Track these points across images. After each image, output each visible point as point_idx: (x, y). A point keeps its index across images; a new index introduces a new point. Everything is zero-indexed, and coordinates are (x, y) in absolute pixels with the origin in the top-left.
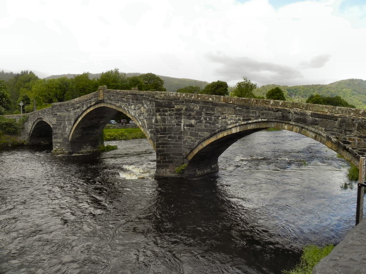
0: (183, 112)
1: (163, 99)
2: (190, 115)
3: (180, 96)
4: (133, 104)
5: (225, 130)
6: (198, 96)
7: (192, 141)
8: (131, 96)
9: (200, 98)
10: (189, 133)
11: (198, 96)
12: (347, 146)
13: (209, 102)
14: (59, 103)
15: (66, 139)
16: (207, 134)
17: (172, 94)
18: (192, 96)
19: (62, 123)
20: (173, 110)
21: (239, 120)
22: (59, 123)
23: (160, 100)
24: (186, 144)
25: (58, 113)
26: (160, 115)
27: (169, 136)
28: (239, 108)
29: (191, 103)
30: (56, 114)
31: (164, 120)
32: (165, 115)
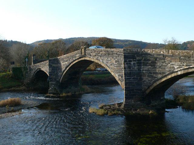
0: (142, 61)
1: (128, 53)
2: (147, 63)
3: (140, 51)
5: (173, 72)
7: (149, 81)
9: (154, 52)
11: (153, 51)
13: (160, 54)
15: (58, 82)
17: (135, 50)
21: (183, 65)
23: (127, 54)
24: (145, 83)
27: (133, 78)
29: (148, 55)
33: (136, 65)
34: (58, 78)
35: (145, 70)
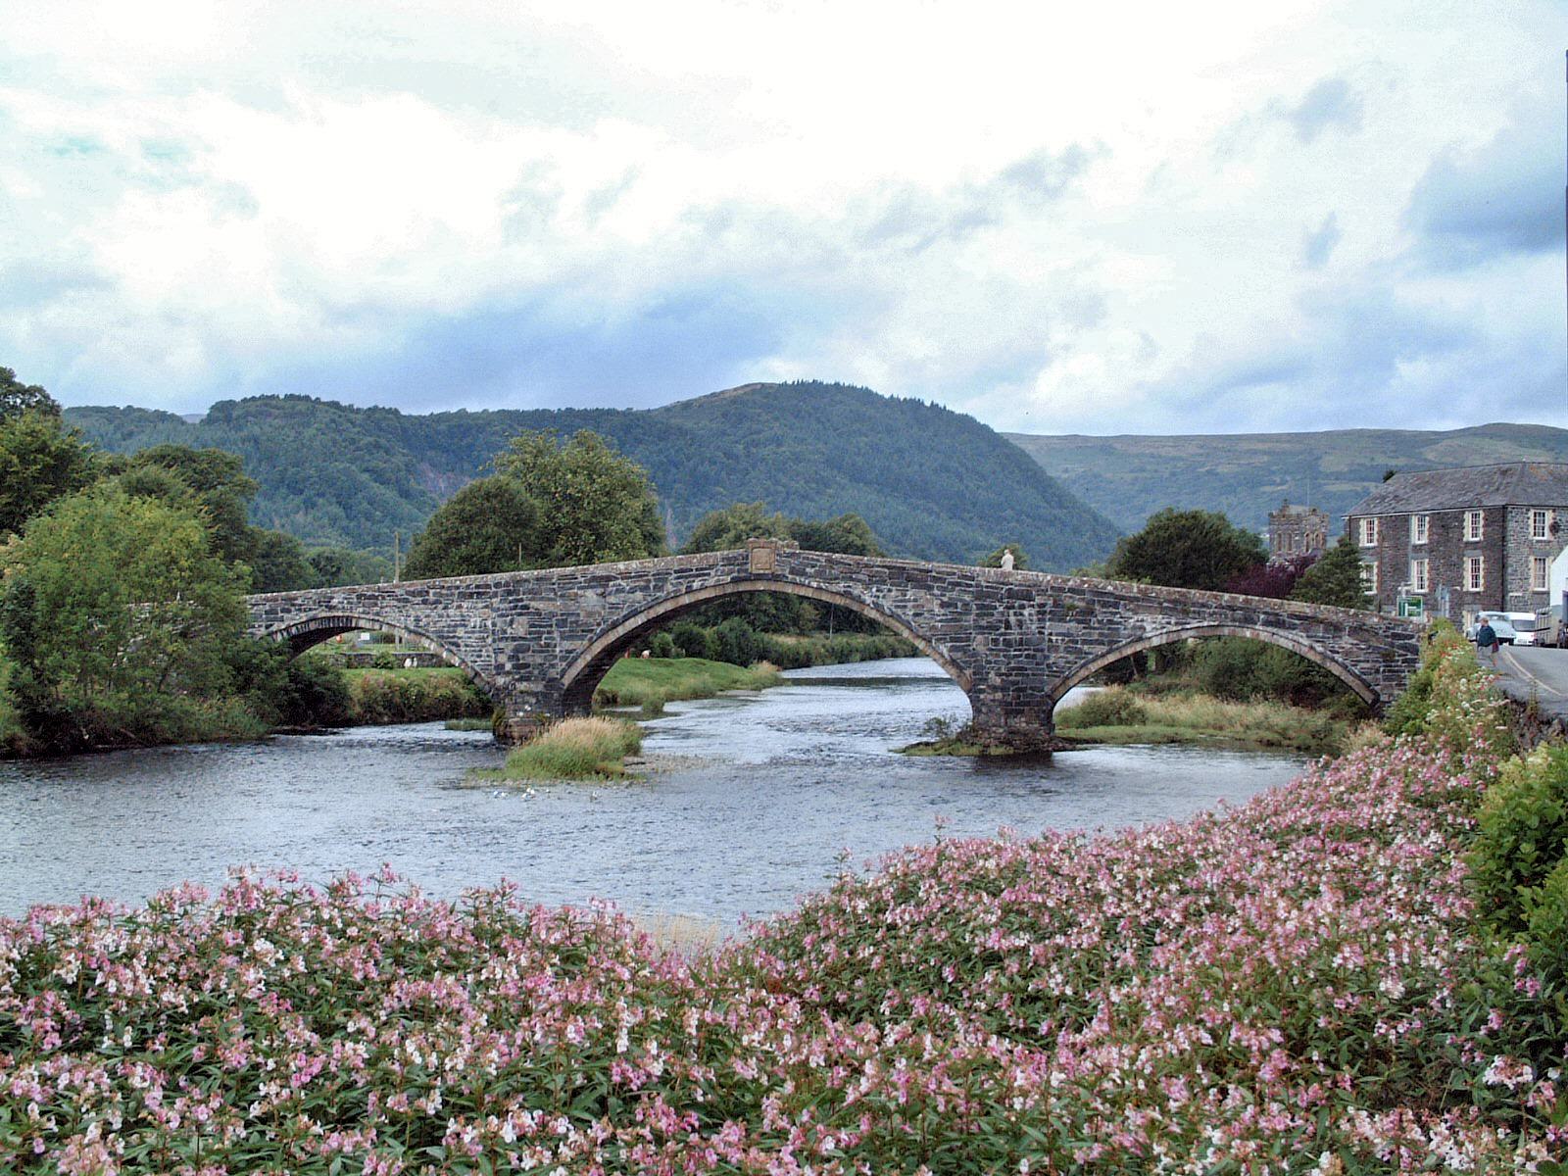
0: (1047, 608)
5: (1140, 639)
6: (1084, 582)
10: (1062, 649)
11: (1084, 582)
12: (1336, 656)
14: (536, 573)
15: (552, 683)
16: (1105, 649)
18: (1069, 580)
19: (544, 633)
20: (1033, 606)
21: (1169, 623)
22: (535, 633)
25: (533, 604)
26: (1015, 614)
30: (526, 607)
31: (1020, 624)
32: (1021, 614)
33: (1035, 618)
34: (553, 666)
35: (1057, 635)
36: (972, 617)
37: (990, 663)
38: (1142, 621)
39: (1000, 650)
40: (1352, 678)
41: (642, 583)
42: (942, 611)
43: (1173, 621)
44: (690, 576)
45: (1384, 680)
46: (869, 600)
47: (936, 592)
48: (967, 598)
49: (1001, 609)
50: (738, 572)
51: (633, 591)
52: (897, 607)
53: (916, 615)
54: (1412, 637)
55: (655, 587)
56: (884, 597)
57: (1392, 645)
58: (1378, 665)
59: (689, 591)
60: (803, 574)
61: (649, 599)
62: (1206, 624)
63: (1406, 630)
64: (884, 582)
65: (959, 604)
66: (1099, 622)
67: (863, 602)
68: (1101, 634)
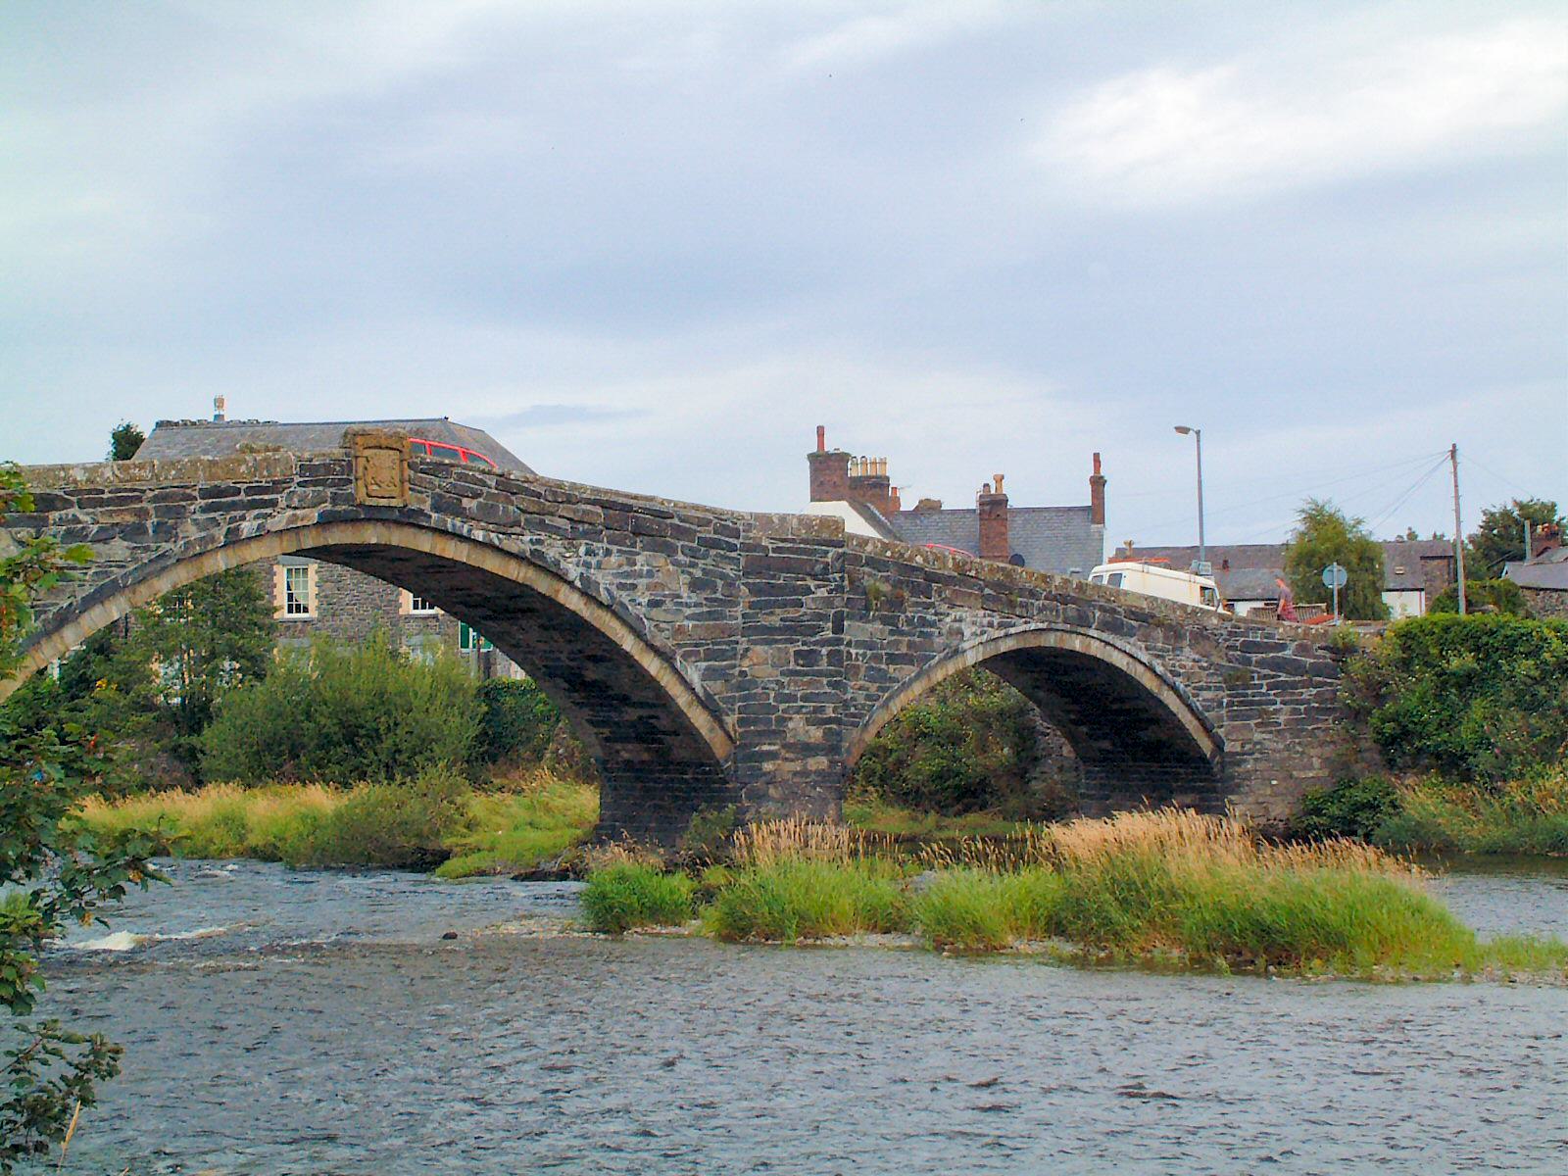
4: (615, 548)
7: (868, 697)
8: (599, 510)
9: (889, 554)
21: (991, 625)
24: (852, 710)
28: (991, 592)
35: (859, 644)
36: (740, 610)
37: (791, 698)
38: (960, 621)
39: (820, 674)
40: (1189, 716)
41: (130, 519)
42: (694, 598)
43: (996, 621)
44: (233, 506)
45: (1232, 718)
46: (574, 573)
47: (680, 557)
48: (729, 570)
49: (822, 593)
50: (335, 499)
51: (105, 536)
52: (621, 587)
53: (654, 604)
54: (1283, 647)
55: (158, 527)
56: (599, 566)
57: (1249, 662)
58: (1222, 694)
59: (233, 539)
60: (459, 512)
61: (145, 557)
62: (1033, 626)
63: (1270, 636)
64: (593, 535)
65: (720, 583)
66: (910, 622)
67: (560, 577)
68: (910, 645)
